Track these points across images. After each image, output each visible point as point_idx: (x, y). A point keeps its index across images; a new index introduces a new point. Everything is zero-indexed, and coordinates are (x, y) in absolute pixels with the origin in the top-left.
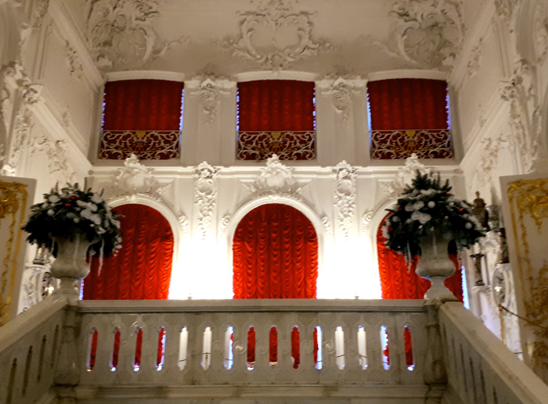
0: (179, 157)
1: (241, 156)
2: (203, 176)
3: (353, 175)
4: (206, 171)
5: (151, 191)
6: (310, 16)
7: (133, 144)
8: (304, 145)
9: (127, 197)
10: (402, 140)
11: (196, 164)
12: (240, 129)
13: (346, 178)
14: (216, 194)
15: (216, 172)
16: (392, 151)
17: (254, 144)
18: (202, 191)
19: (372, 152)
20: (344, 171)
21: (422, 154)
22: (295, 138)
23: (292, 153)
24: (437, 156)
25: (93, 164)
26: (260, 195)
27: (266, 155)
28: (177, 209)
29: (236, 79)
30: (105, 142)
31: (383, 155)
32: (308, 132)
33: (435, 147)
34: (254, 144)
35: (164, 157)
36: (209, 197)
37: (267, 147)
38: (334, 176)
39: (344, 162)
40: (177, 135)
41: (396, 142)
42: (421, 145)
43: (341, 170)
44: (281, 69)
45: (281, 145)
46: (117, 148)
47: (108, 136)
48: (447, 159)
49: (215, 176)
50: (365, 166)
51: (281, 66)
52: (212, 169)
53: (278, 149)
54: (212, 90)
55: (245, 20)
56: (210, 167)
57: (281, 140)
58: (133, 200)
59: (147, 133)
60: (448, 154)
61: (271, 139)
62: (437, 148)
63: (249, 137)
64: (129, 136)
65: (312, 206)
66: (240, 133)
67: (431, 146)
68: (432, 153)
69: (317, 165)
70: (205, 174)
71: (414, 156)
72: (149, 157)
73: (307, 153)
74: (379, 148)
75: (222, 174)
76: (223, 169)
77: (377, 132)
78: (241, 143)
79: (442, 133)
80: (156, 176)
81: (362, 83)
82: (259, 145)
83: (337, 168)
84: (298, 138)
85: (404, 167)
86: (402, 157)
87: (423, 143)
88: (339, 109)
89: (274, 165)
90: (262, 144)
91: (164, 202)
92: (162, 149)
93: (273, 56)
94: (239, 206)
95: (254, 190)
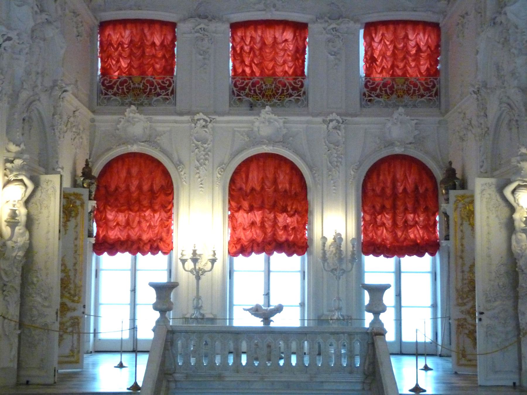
2: (198, 125)
3: (343, 126)
4: (202, 121)
5: (149, 140)
9: (129, 146)
13: (335, 128)
17: (247, 90)
25: (93, 112)
28: (176, 159)
30: (102, 88)
34: (247, 90)
36: (205, 146)
37: (260, 93)
39: (334, 114)
40: (171, 80)
41: (386, 91)
43: (331, 121)
44: (273, 10)
45: (274, 91)
47: (106, 82)
49: (210, 125)
51: (274, 6)
53: (270, 96)
54: (206, 33)
56: (205, 117)
57: (273, 86)
58: (135, 149)
59: (143, 78)
61: (263, 85)
66: (234, 78)
69: (308, 114)
76: (218, 118)
79: (431, 81)
80: (154, 125)
82: (252, 91)
89: (268, 116)
90: (255, 90)
94: (234, 156)
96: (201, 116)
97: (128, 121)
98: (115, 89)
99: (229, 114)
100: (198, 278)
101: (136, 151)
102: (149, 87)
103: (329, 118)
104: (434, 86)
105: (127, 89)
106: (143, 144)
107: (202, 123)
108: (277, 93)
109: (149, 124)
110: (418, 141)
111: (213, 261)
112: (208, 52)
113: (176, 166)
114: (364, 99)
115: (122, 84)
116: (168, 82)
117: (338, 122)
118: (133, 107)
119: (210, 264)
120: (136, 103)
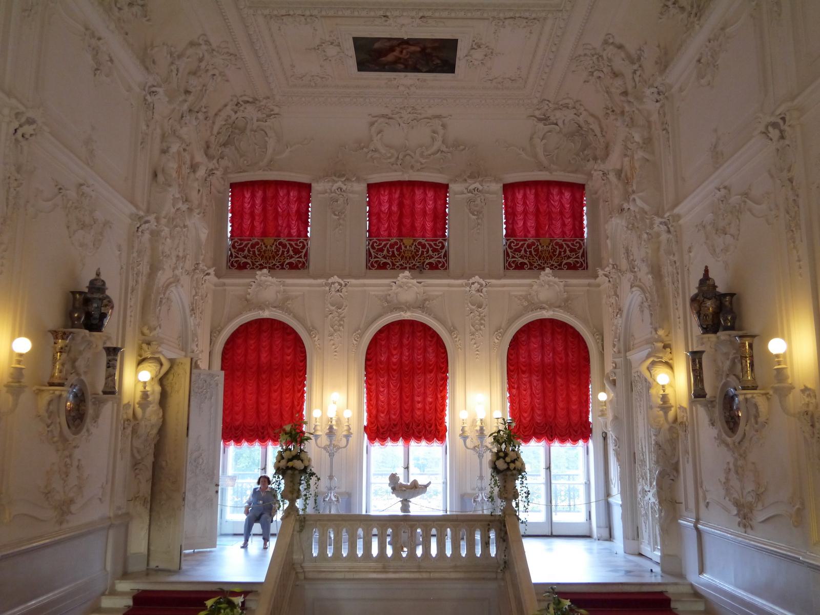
0: (308, 267)
1: (373, 266)
2: (333, 289)
4: (337, 284)
6: (444, 120)
7: (261, 252)
8: (437, 253)
10: (537, 250)
11: (328, 277)
12: (369, 236)
13: (478, 291)
14: (347, 308)
15: (346, 285)
16: (526, 261)
18: (333, 306)
19: (505, 261)
20: (476, 284)
21: (556, 264)
22: (428, 246)
23: (424, 262)
24: (571, 267)
26: (392, 311)
27: (398, 264)
29: (365, 180)
31: (516, 265)
32: (441, 240)
33: (569, 257)
35: (293, 266)
38: (468, 288)
39: (477, 277)
40: (305, 242)
41: (530, 252)
42: (555, 255)
43: (473, 283)
46: (245, 257)
48: (580, 272)
49: (344, 289)
50: (499, 278)
52: (342, 282)
55: (376, 121)
56: (340, 281)
58: (266, 314)
60: (582, 264)
62: (571, 259)
63: (380, 244)
64: (257, 243)
65: (443, 323)
66: (370, 240)
67: (566, 256)
68: (566, 264)
70: (335, 288)
71: (548, 270)
72: (278, 267)
73: (440, 262)
74: (513, 257)
75: (351, 286)
77: (512, 239)
78: (372, 251)
79: (577, 243)
80: (288, 288)
81: (497, 187)
83: (471, 281)
84: (430, 245)
85: (538, 281)
86: (535, 267)
87: (557, 253)
88: (474, 215)
91: (296, 317)
92: (292, 258)
93: (405, 156)
95: (386, 305)
96: (335, 279)
97: (260, 285)
98: (246, 252)
99: (364, 277)
100: (331, 455)
101: (268, 317)
102: (281, 250)
103: (471, 281)
104: (580, 247)
105: (259, 251)
106: (274, 309)
107: (337, 286)
108: (417, 255)
109: (282, 288)
110: (566, 304)
111: (348, 437)
112: (344, 213)
113: (309, 332)
114: (507, 261)
115: (253, 246)
116: (301, 244)
117: (481, 285)
118: (265, 271)
119: (344, 440)
120: (268, 265)
